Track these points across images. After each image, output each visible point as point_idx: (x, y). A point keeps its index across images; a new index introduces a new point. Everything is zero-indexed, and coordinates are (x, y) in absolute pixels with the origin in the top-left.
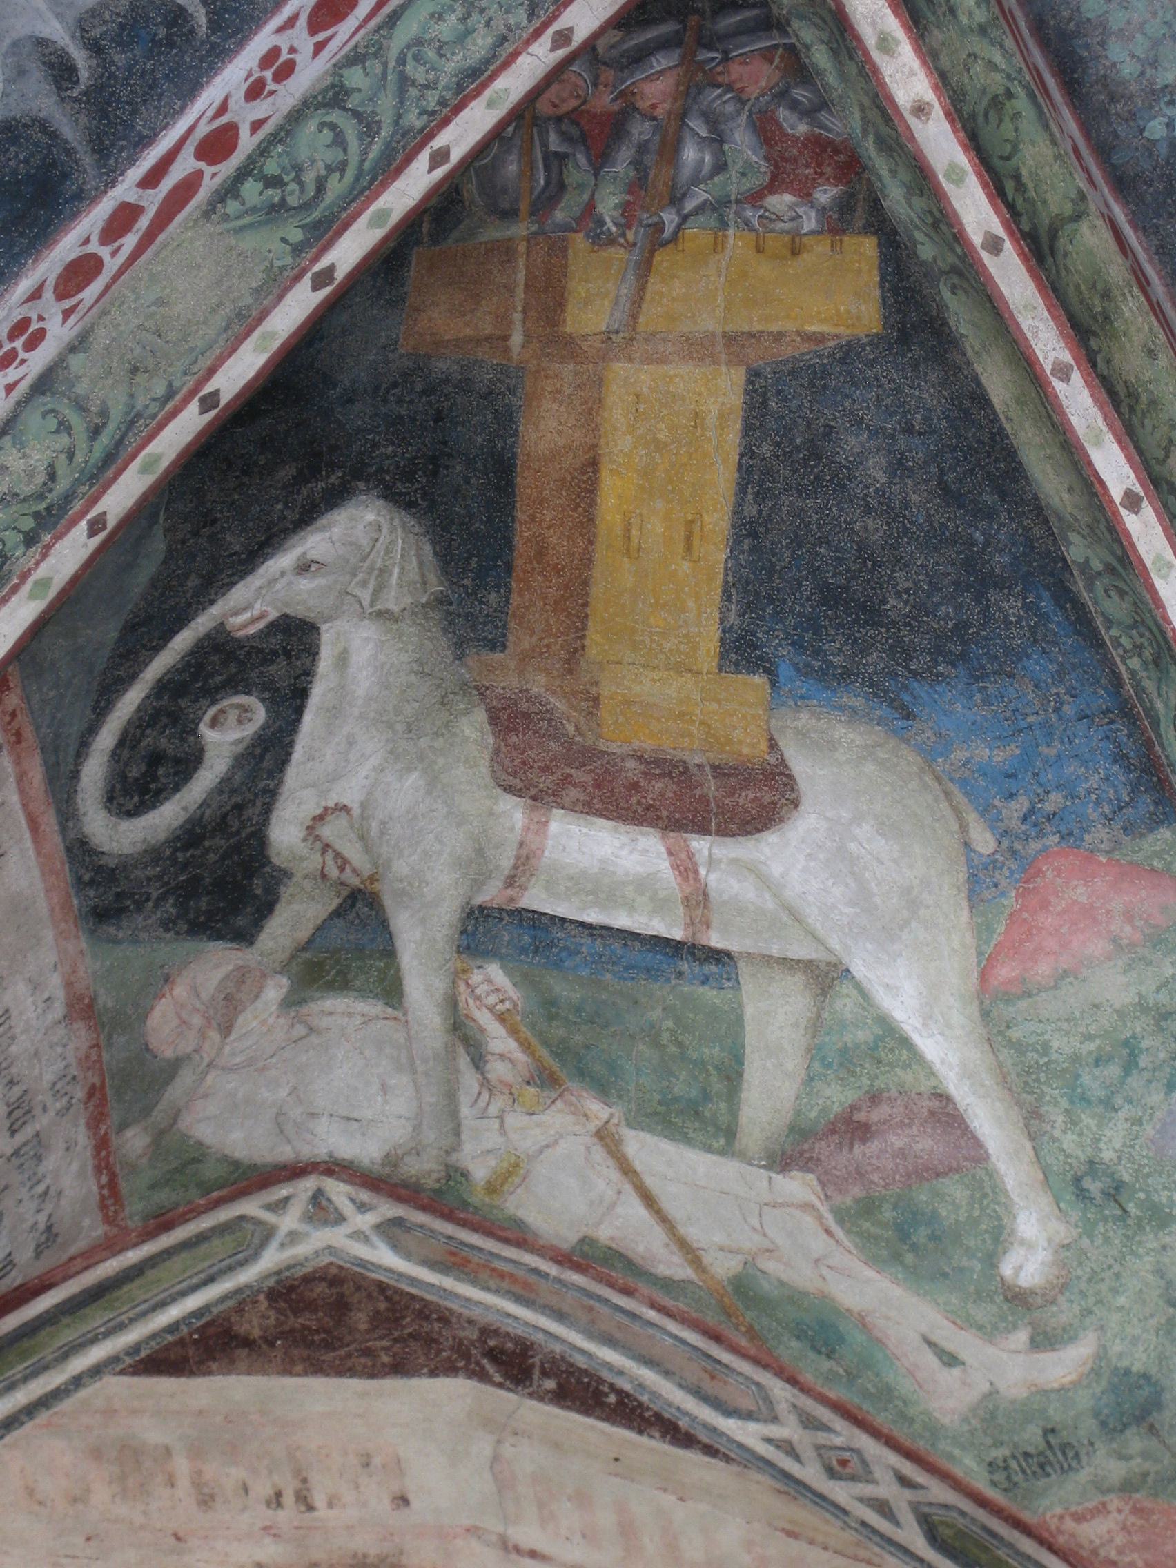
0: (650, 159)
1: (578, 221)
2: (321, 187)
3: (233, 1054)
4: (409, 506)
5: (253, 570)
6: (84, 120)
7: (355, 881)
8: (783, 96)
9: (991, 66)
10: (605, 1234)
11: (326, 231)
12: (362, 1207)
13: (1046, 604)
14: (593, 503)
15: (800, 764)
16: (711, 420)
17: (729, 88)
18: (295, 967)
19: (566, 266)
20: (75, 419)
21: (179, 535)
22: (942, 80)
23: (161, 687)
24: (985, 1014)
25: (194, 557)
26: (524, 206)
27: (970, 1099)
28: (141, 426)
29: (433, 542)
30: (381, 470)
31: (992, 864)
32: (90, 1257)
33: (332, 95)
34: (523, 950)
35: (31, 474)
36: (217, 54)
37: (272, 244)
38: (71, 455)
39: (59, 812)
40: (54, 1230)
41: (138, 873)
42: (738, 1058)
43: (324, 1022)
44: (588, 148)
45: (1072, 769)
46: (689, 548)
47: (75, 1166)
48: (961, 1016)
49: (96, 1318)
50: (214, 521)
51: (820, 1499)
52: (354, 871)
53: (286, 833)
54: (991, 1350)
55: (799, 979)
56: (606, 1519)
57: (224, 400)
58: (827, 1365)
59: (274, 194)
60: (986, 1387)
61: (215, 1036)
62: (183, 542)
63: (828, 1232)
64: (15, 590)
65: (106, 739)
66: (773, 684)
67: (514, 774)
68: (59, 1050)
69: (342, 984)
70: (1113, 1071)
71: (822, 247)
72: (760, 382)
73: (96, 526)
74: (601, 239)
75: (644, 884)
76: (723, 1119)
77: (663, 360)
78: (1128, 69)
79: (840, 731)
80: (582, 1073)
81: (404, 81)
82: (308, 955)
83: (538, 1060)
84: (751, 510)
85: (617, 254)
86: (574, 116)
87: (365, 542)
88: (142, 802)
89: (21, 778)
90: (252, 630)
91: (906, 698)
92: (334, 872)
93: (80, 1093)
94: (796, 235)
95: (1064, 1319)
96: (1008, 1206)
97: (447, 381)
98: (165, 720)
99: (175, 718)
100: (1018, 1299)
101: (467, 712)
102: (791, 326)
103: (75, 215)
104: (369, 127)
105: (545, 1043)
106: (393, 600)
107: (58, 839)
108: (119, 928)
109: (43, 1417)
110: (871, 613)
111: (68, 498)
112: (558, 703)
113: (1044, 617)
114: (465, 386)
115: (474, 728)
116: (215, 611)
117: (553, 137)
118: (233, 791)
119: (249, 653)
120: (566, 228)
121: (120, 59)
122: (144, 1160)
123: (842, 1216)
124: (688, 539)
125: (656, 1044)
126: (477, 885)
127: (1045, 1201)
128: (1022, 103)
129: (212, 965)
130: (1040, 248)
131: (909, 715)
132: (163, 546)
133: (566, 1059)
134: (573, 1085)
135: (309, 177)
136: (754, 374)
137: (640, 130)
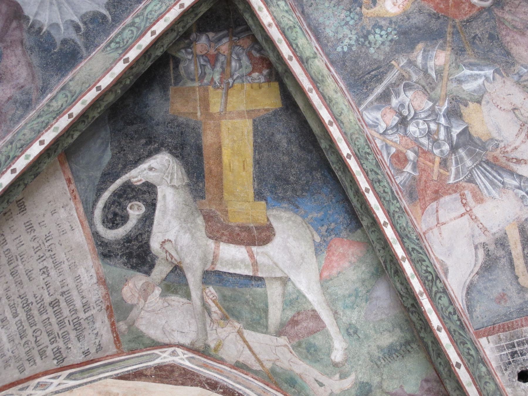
0: (225, 66)
1: (210, 82)
2: (127, 42)
3: (148, 307)
4: (177, 157)
5: (137, 167)
6: (82, 40)
7: (176, 263)
8: (252, 47)
10: (241, 360)
11: (127, 50)
13: (326, 174)
14: (221, 158)
15: (275, 224)
16: (246, 133)
18: (162, 285)
19: (208, 94)
20: (69, 95)
21: (115, 152)
22: (274, 18)
23: (114, 194)
24: (322, 286)
25: (120, 159)
26: (196, 78)
27: (321, 310)
28: (82, 94)
29: (184, 168)
30: (168, 145)
31: (320, 245)
32: (112, 356)
33: (133, 24)
34: (217, 282)
35: (58, 106)
36: (113, 27)
37: (115, 55)
38: (67, 101)
39: (89, 222)
40: (101, 346)
41: (114, 246)
42: (267, 307)
43: (173, 303)
44: (210, 64)
46: (244, 168)
47: (105, 328)
48: (316, 287)
49: (110, 368)
50: (124, 150)
52: (175, 260)
53: (155, 245)
54: (331, 380)
55: (279, 282)
57: (103, 88)
58: (293, 390)
59: (118, 45)
60: (330, 391)
61: (142, 301)
62: (116, 154)
63: (291, 352)
64: (49, 128)
66: (267, 203)
67: (211, 233)
68: (97, 292)
69: (175, 292)
70: (353, 298)
72: (256, 123)
73: (70, 116)
74: (216, 88)
75: (243, 261)
76: (265, 324)
78: (331, 34)
79: (283, 214)
80: (233, 315)
81: (147, 19)
82: (166, 282)
84: (257, 157)
85: (219, 91)
86: (206, 55)
87: (166, 165)
88: (113, 226)
89: (77, 209)
90: (139, 183)
91: (297, 203)
92: (170, 259)
93: (104, 307)
95: (347, 369)
96: (331, 339)
98: (117, 204)
99: (120, 204)
100: (336, 365)
101: (198, 216)
103: (81, 62)
104: (138, 28)
105: (224, 308)
106: (176, 182)
107: (89, 229)
108: (111, 261)
109: (90, 384)
110: (287, 182)
111: (64, 110)
112: (218, 213)
114: (187, 125)
115: (200, 221)
118: (139, 229)
119: (138, 190)
121: (91, 26)
122: (126, 333)
123: (294, 347)
124: (244, 165)
127: (340, 337)
128: (298, 29)
129: (138, 280)
130: (303, 61)
131: (298, 207)
132: (111, 154)
133: (229, 314)
134: (231, 319)
135: (125, 41)
136: (254, 121)
137: (222, 58)
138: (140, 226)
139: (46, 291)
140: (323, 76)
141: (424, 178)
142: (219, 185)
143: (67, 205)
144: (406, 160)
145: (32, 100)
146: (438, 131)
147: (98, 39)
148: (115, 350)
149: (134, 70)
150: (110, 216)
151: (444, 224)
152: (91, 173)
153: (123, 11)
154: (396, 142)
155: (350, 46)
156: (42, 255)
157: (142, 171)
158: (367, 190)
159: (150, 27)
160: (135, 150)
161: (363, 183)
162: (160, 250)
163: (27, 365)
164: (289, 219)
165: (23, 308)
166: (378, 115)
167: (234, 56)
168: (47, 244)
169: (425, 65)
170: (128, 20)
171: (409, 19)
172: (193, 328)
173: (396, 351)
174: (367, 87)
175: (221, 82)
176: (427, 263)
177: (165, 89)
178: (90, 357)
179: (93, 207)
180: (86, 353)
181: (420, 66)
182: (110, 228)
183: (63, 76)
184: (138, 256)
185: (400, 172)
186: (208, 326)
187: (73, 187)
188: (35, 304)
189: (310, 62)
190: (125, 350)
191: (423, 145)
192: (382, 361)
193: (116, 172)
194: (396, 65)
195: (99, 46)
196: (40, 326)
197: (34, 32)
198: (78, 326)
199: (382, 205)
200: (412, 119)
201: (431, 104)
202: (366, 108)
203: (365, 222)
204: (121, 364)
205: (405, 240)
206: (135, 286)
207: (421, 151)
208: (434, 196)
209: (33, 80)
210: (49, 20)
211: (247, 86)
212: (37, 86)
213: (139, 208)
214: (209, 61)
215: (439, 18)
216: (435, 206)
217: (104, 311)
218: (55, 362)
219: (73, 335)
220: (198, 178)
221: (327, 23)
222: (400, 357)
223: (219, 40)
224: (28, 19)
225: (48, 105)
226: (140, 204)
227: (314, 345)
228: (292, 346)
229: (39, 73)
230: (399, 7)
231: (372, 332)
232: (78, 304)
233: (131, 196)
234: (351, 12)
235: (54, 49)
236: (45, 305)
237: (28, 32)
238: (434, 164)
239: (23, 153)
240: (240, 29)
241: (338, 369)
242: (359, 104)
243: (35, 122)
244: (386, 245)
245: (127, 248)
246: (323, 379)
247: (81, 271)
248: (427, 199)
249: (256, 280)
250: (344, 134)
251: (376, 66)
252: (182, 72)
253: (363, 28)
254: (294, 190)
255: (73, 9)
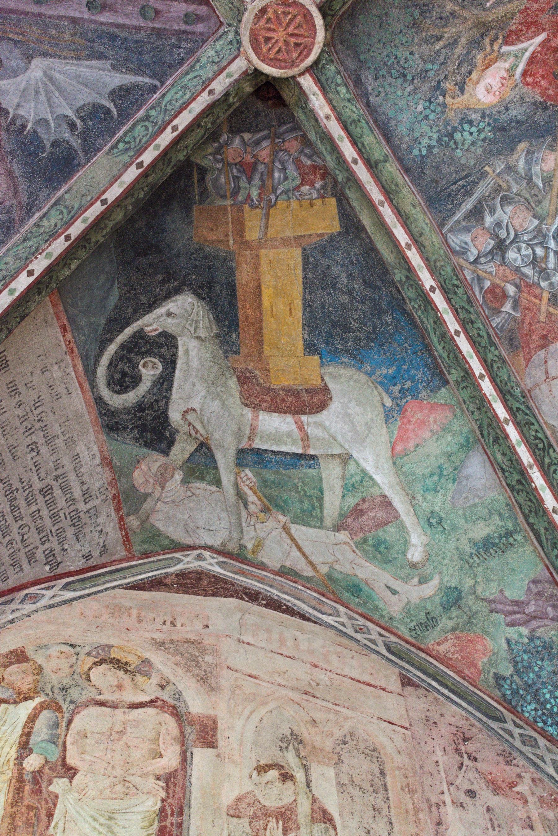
0: (265, 177)
1: (246, 200)
2: (140, 141)
4: (203, 299)
5: (151, 311)
6: (79, 141)
8: (301, 152)
9: (352, 111)
10: (287, 564)
11: (141, 151)
12: (213, 558)
14: (261, 300)
15: (331, 386)
17: (286, 151)
20: (65, 211)
22: (333, 108)
23: (123, 346)
24: (394, 463)
30: (191, 283)
31: (391, 409)
32: (121, 561)
33: (147, 118)
34: (255, 463)
36: (121, 124)
37: (126, 158)
38: (62, 220)
39: (90, 384)
41: (121, 416)
42: (321, 491)
45: (413, 372)
46: (291, 313)
47: (112, 524)
48: (387, 465)
49: (118, 575)
51: (351, 638)
54: (407, 586)
55: (338, 460)
56: (275, 636)
57: (109, 202)
58: (357, 600)
59: (128, 146)
60: (406, 600)
65: (105, 361)
66: (321, 358)
67: (247, 399)
69: (202, 478)
70: (436, 478)
71: (319, 202)
72: (306, 253)
73: (68, 238)
74: (253, 207)
75: (289, 434)
76: (319, 515)
77: (276, 247)
78: (405, 132)
79: (342, 371)
80: (277, 506)
81: (166, 110)
82: (188, 464)
83: (263, 503)
85: (258, 211)
86: (241, 163)
87: (189, 309)
89: (74, 367)
90: (154, 334)
92: (194, 434)
93: (110, 496)
94: (311, 200)
95: (428, 571)
96: (408, 533)
97: (210, 255)
99: (130, 360)
100: (413, 566)
101: (231, 377)
102: (313, 232)
103: (78, 171)
105: (265, 496)
106: (202, 333)
107: (91, 394)
109: (93, 596)
110: (348, 330)
112: (257, 372)
113: (399, 321)
114: (216, 257)
115: (233, 383)
116: (139, 322)
117: (235, 170)
118: (154, 394)
120: (242, 203)
121: (90, 123)
124: (290, 309)
125: (297, 492)
126: (240, 441)
127: (419, 529)
128: (363, 124)
129: (154, 461)
130: (372, 166)
133: (272, 504)
134: (274, 511)
135: (137, 141)
136: (304, 250)
137: (261, 168)
138: (155, 390)
139: (35, 474)
140: (397, 185)
141: (528, 320)
142: (258, 337)
143: (62, 361)
144: (505, 296)
145: (14, 220)
146: (546, 258)
147: (99, 141)
148: (124, 553)
149: (150, 179)
150: (117, 377)
151: (554, 378)
152: (93, 319)
153: (132, 103)
154: (491, 273)
155: (430, 148)
156: (29, 427)
157: (159, 317)
158: (457, 333)
159: (171, 121)
160: (149, 289)
161: (452, 324)
162: (181, 422)
163: (11, 571)
164: (350, 378)
165: (6, 496)
166: (467, 238)
167: (277, 164)
168: (36, 412)
169: (528, 171)
170: (141, 113)
171: (507, 109)
172: (224, 524)
173: (494, 544)
174: (453, 201)
175: (260, 200)
176: (536, 427)
177: (187, 209)
178: (92, 562)
179: (95, 364)
180: (88, 557)
181: (522, 172)
182: (118, 392)
183: (55, 189)
184: (154, 430)
185: (497, 312)
186: (243, 520)
187: (69, 336)
188: (21, 491)
189: (380, 167)
190: (137, 554)
191: (527, 277)
192: (476, 558)
193: (124, 318)
194: (491, 172)
195: (101, 149)
196: (27, 520)
197: (15, 131)
198: (76, 521)
199: (477, 352)
200: (512, 242)
201: (536, 222)
202: (451, 230)
203: (454, 376)
204: (133, 570)
205: (508, 397)
206: (149, 469)
207: (524, 284)
208: (541, 342)
209: (15, 194)
210: (35, 114)
211: (294, 204)
212: (20, 203)
213: (154, 366)
214: (244, 172)
215: (547, 108)
216: (543, 356)
217: (110, 501)
218: (47, 568)
219: (70, 533)
220: (229, 327)
221: (400, 117)
222: (500, 552)
223: (258, 143)
224: (8, 113)
225: (37, 225)
226: (156, 360)
227: (385, 541)
228: (355, 543)
229: (23, 185)
230: (494, 95)
231: (462, 521)
232: (77, 493)
233: (143, 349)
234: (431, 103)
235: (42, 153)
236: (35, 492)
237: (8, 130)
238: (540, 300)
239: (6, 287)
240: (284, 128)
241: (418, 572)
242: (441, 225)
243: (21, 247)
244: (483, 403)
245: (140, 419)
246: (396, 585)
247: (80, 448)
248: (532, 346)
249: (306, 459)
250: (426, 260)
251: (464, 174)
252: (210, 186)
253: (447, 123)
254: (357, 340)
255: (66, 100)
